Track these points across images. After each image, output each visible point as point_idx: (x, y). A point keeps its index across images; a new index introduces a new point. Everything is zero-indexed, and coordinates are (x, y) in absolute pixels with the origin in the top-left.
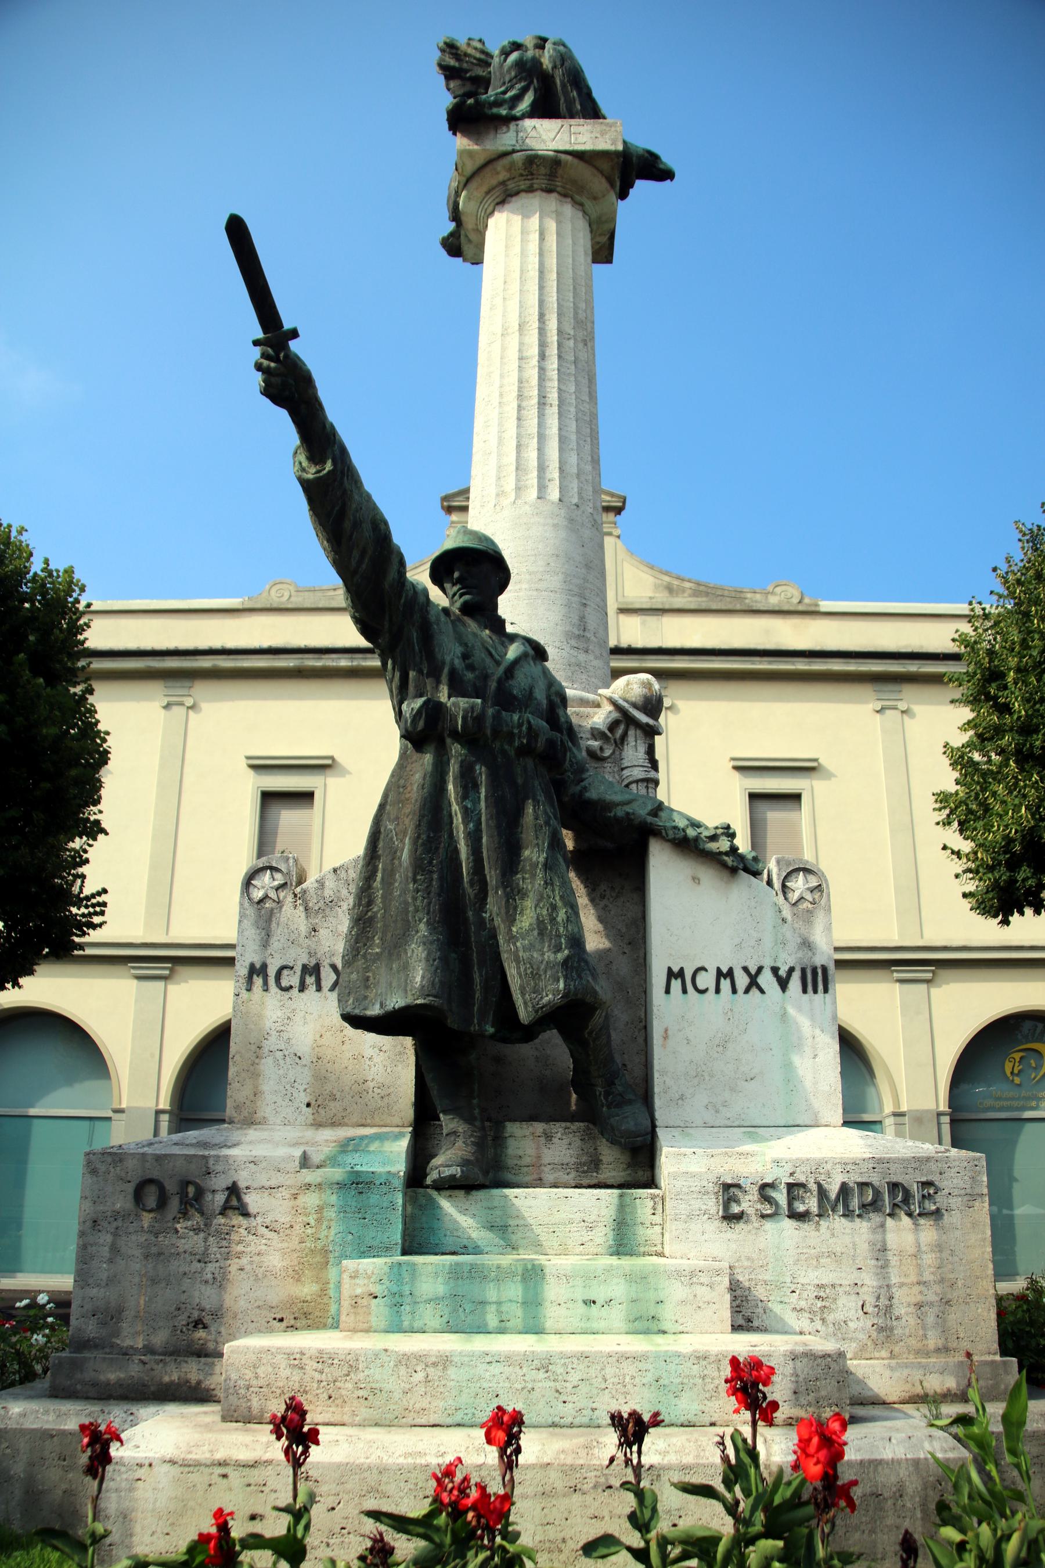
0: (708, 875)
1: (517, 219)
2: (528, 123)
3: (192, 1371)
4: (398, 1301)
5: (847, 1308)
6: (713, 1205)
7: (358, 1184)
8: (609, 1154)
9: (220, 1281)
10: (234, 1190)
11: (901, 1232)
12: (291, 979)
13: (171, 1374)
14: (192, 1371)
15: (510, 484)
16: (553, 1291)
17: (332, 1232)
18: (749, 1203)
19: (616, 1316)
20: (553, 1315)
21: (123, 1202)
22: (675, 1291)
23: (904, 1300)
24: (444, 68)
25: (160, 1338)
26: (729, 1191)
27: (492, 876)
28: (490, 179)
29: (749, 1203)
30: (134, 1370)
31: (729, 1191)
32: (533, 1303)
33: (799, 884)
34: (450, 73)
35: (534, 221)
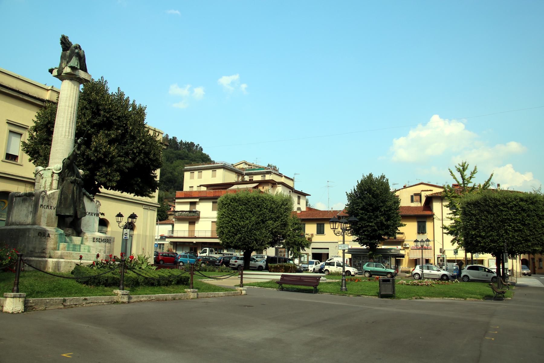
0: (89, 201)
1: (73, 85)
2: (80, 71)
3: (44, 255)
4: (68, 247)
5: (102, 251)
6: (92, 240)
7: (61, 234)
8: (75, 233)
9: (46, 245)
10: (49, 234)
11: (107, 244)
12: (45, 207)
13: (42, 255)
14: (44, 255)
15: (67, 134)
16: (82, 247)
17: (58, 240)
18: (95, 240)
19: (87, 251)
20: (82, 250)
21: (37, 235)
22: (92, 248)
23: (107, 251)
24: (61, 40)
25: (40, 251)
26: (94, 238)
27: (78, 200)
28: (71, 76)
29: (95, 240)
30: (38, 254)
31: (94, 238)
32: (80, 249)
33: (98, 203)
34: (62, 43)
35: (76, 87)
